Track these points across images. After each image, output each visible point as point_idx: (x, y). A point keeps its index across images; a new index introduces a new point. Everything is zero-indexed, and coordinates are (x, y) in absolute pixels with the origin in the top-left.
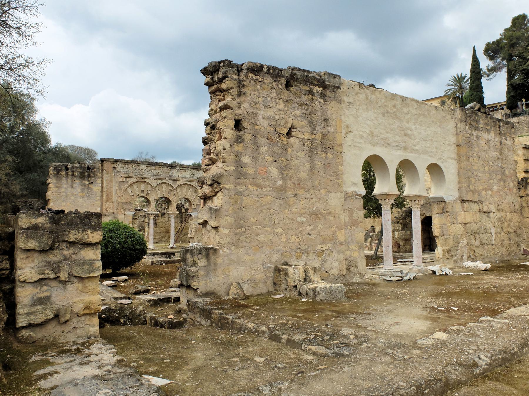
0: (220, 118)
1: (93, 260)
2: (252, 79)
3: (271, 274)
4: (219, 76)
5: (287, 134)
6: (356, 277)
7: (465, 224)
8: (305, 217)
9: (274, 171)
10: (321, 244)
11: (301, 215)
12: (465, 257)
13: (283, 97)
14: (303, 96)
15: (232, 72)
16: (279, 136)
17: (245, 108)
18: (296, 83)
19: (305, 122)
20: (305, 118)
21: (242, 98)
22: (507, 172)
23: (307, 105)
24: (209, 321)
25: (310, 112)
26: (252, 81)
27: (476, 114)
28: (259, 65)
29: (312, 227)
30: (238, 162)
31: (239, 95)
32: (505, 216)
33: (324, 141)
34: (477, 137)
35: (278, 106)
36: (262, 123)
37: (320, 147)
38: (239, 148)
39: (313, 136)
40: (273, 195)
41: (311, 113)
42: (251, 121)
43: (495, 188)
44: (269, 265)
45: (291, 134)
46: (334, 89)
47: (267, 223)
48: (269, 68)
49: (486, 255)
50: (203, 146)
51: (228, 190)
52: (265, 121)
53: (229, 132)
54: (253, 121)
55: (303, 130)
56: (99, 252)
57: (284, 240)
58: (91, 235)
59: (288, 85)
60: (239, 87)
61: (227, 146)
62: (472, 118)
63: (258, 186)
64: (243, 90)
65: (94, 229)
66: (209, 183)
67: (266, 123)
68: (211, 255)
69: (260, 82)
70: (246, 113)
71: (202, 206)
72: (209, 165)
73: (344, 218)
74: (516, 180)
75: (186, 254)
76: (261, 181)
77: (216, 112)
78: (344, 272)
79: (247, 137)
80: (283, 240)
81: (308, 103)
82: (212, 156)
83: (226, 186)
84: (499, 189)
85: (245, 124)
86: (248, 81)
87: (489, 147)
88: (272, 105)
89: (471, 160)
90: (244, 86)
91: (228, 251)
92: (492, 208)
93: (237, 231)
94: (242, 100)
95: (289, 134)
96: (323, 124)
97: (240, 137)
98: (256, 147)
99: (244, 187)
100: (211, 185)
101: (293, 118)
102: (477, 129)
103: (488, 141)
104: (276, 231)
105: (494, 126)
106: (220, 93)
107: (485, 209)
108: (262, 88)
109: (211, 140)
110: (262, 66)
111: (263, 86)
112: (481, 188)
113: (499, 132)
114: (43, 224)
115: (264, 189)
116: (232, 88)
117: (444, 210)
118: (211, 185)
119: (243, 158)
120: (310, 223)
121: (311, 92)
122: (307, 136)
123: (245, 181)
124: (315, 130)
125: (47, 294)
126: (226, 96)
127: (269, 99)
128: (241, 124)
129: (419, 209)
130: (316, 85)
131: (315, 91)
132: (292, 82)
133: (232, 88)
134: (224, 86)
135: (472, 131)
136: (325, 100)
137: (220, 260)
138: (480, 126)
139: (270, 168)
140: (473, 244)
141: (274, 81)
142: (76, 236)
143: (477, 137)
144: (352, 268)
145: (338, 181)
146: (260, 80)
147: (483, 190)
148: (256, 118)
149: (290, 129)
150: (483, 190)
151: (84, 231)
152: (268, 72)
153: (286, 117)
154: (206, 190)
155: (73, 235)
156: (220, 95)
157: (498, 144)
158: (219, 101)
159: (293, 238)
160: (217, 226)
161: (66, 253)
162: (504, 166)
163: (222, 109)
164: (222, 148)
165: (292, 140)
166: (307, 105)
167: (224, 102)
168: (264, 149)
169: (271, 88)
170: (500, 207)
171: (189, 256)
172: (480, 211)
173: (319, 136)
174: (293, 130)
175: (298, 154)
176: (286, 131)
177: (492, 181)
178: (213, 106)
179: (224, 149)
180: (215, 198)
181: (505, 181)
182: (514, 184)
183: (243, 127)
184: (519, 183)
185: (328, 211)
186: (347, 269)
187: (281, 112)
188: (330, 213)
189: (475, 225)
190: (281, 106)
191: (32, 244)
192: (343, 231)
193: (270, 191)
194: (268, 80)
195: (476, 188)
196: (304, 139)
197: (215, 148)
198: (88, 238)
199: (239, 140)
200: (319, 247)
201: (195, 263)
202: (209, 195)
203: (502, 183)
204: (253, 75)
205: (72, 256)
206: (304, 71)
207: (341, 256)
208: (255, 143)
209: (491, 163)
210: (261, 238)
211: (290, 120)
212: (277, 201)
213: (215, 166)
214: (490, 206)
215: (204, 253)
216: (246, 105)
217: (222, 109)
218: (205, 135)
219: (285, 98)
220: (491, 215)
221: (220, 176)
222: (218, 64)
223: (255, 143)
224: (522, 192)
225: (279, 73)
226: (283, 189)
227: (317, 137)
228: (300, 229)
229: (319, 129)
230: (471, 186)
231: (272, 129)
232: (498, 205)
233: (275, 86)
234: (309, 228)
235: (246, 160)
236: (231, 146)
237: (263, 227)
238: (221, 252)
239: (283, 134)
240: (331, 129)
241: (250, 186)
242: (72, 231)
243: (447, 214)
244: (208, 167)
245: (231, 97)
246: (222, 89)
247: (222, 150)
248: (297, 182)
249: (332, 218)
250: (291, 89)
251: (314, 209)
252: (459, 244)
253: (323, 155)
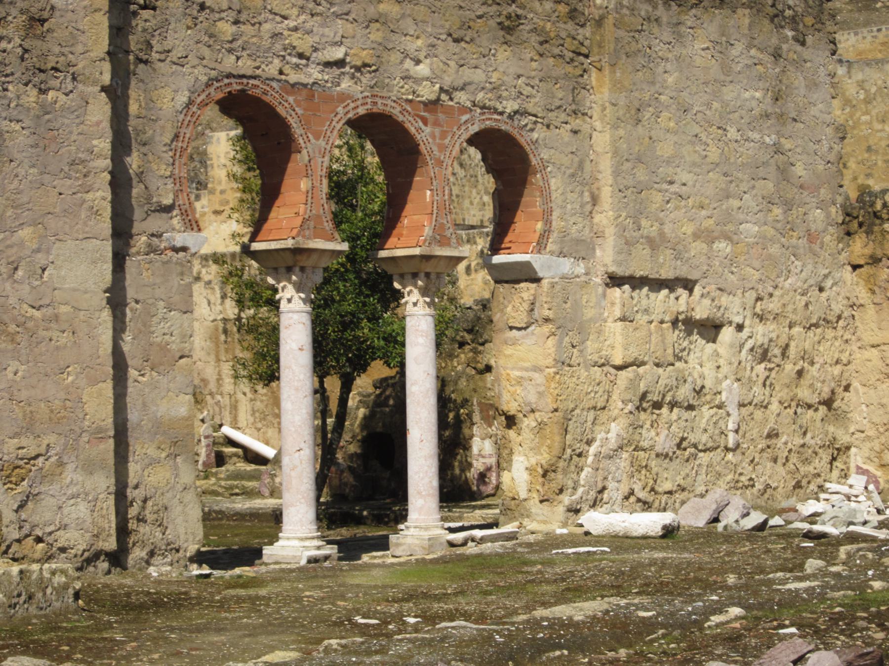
10: (16, 435)
22: (799, 170)
43: (750, 229)
74: (840, 200)
87: (726, 69)
92: (734, 308)
107: (700, 314)
112: (689, 229)
117: (536, 314)
135: (655, 7)
140: (645, 444)
147: (696, 236)
150: (696, 236)
177: (735, 203)
182: (828, 215)
185: (49, 311)
188: (56, 318)
195: (667, 229)
203: (777, 211)
214: (725, 300)
230: (644, 223)
252: (589, 443)
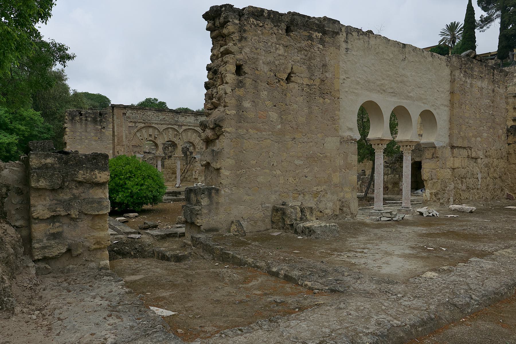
0: (222, 63)
1: (101, 198)
2: (253, 24)
3: (269, 213)
4: (220, 21)
5: (286, 79)
6: (348, 216)
7: (454, 169)
8: (302, 160)
9: (274, 115)
10: (317, 186)
11: (299, 158)
12: (452, 200)
13: (283, 42)
14: (303, 42)
15: (233, 17)
16: (279, 81)
17: (246, 53)
18: (296, 28)
20: (304, 63)
21: (243, 43)
22: (497, 120)
23: (306, 50)
24: (212, 255)
25: (309, 58)
26: (253, 26)
27: (472, 62)
28: (260, 10)
30: (239, 107)
31: (240, 40)
32: (492, 162)
33: (322, 87)
34: (471, 85)
35: (278, 52)
36: (262, 68)
37: (318, 93)
38: (240, 92)
40: (272, 139)
41: (310, 59)
42: (251, 66)
44: (267, 205)
45: (290, 79)
46: (333, 35)
47: (266, 166)
48: (270, 12)
49: (471, 199)
50: (205, 91)
51: (229, 133)
52: (265, 66)
53: (230, 77)
54: (253, 66)
55: (302, 75)
56: (107, 191)
57: (282, 181)
58: (98, 175)
59: (288, 30)
60: (240, 32)
61: (229, 90)
62: (467, 66)
63: (258, 130)
64: (245, 35)
65: (103, 169)
66: (211, 126)
67: (266, 69)
68: (213, 194)
69: (261, 27)
70: (247, 58)
71: (204, 149)
72: (211, 110)
73: (340, 162)
74: (506, 127)
75: (190, 193)
76: (261, 124)
77: (217, 58)
78: (338, 213)
79: (248, 82)
80: (280, 182)
81: (307, 49)
82: (214, 100)
83: (228, 130)
84: (488, 136)
85: (246, 69)
86: (249, 26)
87: (482, 94)
88: (272, 50)
89: (463, 106)
90: (245, 31)
91: (229, 192)
92: (481, 154)
93: (238, 172)
94: (243, 45)
96: (321, 70)
97: (241, 82)
98: (256, 92)
99: (245, 130)
100: (213, 129)
101: (293, 63)
102: (472, 76)
104: (275, 173)
105: (488, 74)
106: (222, 39)
108: (263, 33)
109: (213, 85)
110: (262, 10)
111: (264, 31)
113: (492, 80)
114: (52, 165)
115: (264, 133)
116: (233, 33)
118: (213, 129)
119: (244, 102)
120: (306, 166)
121: (310, 38)
122: (306, 81)
123: (246, 124)
124: (314, 75)
125: (60, 230)
126: (227, 41)
127: (269, 44)
128: (242, 69)
129: (410, 154)
130: (316, 31)
131: (314, 36)
132: (292, 28)
133: (233, 33)
134: (225, 31)
136: (324, 46)
137: (222, 200)
138: (475, 73)
139: (270, 113)
140: (459, 188)
141: (275, 26)
142: (84, 176)
143: (471, 85)
144: (345, 209)
145: (334, 126)
146: (261, 25)
148: (257, 63)
149: (289, 74)
151: (92, 170)
152: (269, 17)
153: (286, 62)
154: (209, 133)
155: (81, 175)
156: (222, 40)
157: (491, 92)
158: (221, 46)
159: (291, 179)
160: (219, 167)
161: (75, 191)
162: (495, 113)
163: (223, 54)
164: (223, 92)
165: (291, 85)
166: (306, 50)
167: (226, 47)
168: (264, 94)
169: (272, 33)
170: (488, 153)
171: (192, 195)
172: (468, 157)
173: (317, 82)
174: (292, 75)
175: (297, 99)
176: (286, 76)
178: (215, 52)
179: (226, 93)
180: (217, 141)
181: (494, 128)
182: (503, 131)
183: (244, 72)
184: (508, 130)
185: (324, 155)
186: (340, 209)
187: (281, 57)
188: (326, 156)
189: (463, 170)
190: (281, 51)
191: (42, 183)
192: (338, 174)
193: (269, 135)
194: (269, 25)
196: (303, 84)
197: (217, 92)
198: (96, 178)
199: (240, 84)
200: (315, 189)
201: (198, 203)
202: (211, 138)
204: (254, 20)
205: (82, 195)
206: (304, 16)
207: (335, 198)
208: (256, 87)
209: (482, 111)
210: (261, 179)
211: (290, 66)
212: (276, 144)
213: (216, 110)
214: (478, 152)
215: (206, 193)
216: (247, 50)
217: (223, 54)
218: (207, 80)
219: (284, 43)
220: (479, 161)
221: (222, 120)
222: (219, 8)
223: (256, 87)
224: (511, 139)
225: (279, 18)
227: (315, 83)
228: (297, 172)
229: (318, 74)
230: (461, 133)
231: (272, 74)
232: (486, 152)
233: (276, 31)
234: (306, 170)
235: (247, 104)
236: (232, 90)
237: (263, 169)
238: (223, 192)
241: (250, 130)
242: (80, 171)
243: (437, 159)
244: (210, 112)
245: (232, 42)
246: (224, 34)
247: (224, 95)
248: (295, 126)
249: (327, 162)
250: (291, 34)
251: (311, 152)
252: (446, 187)
253: (321, 100)
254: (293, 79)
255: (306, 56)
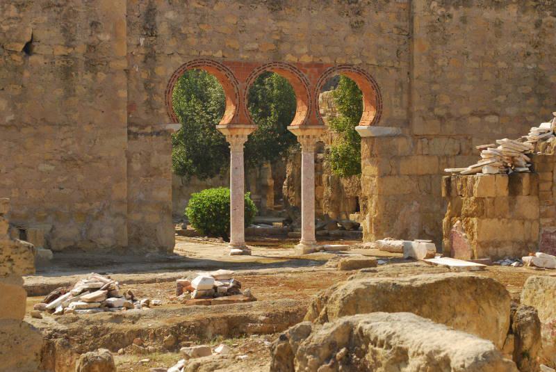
8: (52, 165)
10: (82, 203)
11: (47, 161)
19: (55, 32)
29: (65, 178)
35: (7, 13)
39: (70, 50)
95: (28, 49)
96: (89, 31)
103: (498, 24)
112: (466, 110)
122: (61, 51)
150: (472, 114)
157: (531, 27)
165: (32, 59)
211: (29, 31)
226: (16, 125)
239: (16, 52)
240: (105, 37)
253: (88, 77)
254: (35, 50)
255: (59, 13)
